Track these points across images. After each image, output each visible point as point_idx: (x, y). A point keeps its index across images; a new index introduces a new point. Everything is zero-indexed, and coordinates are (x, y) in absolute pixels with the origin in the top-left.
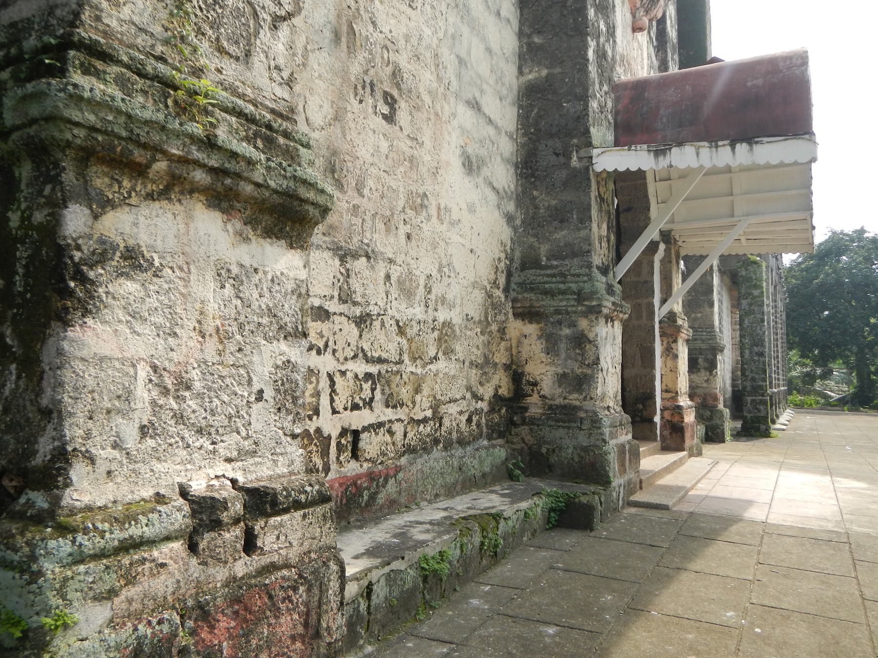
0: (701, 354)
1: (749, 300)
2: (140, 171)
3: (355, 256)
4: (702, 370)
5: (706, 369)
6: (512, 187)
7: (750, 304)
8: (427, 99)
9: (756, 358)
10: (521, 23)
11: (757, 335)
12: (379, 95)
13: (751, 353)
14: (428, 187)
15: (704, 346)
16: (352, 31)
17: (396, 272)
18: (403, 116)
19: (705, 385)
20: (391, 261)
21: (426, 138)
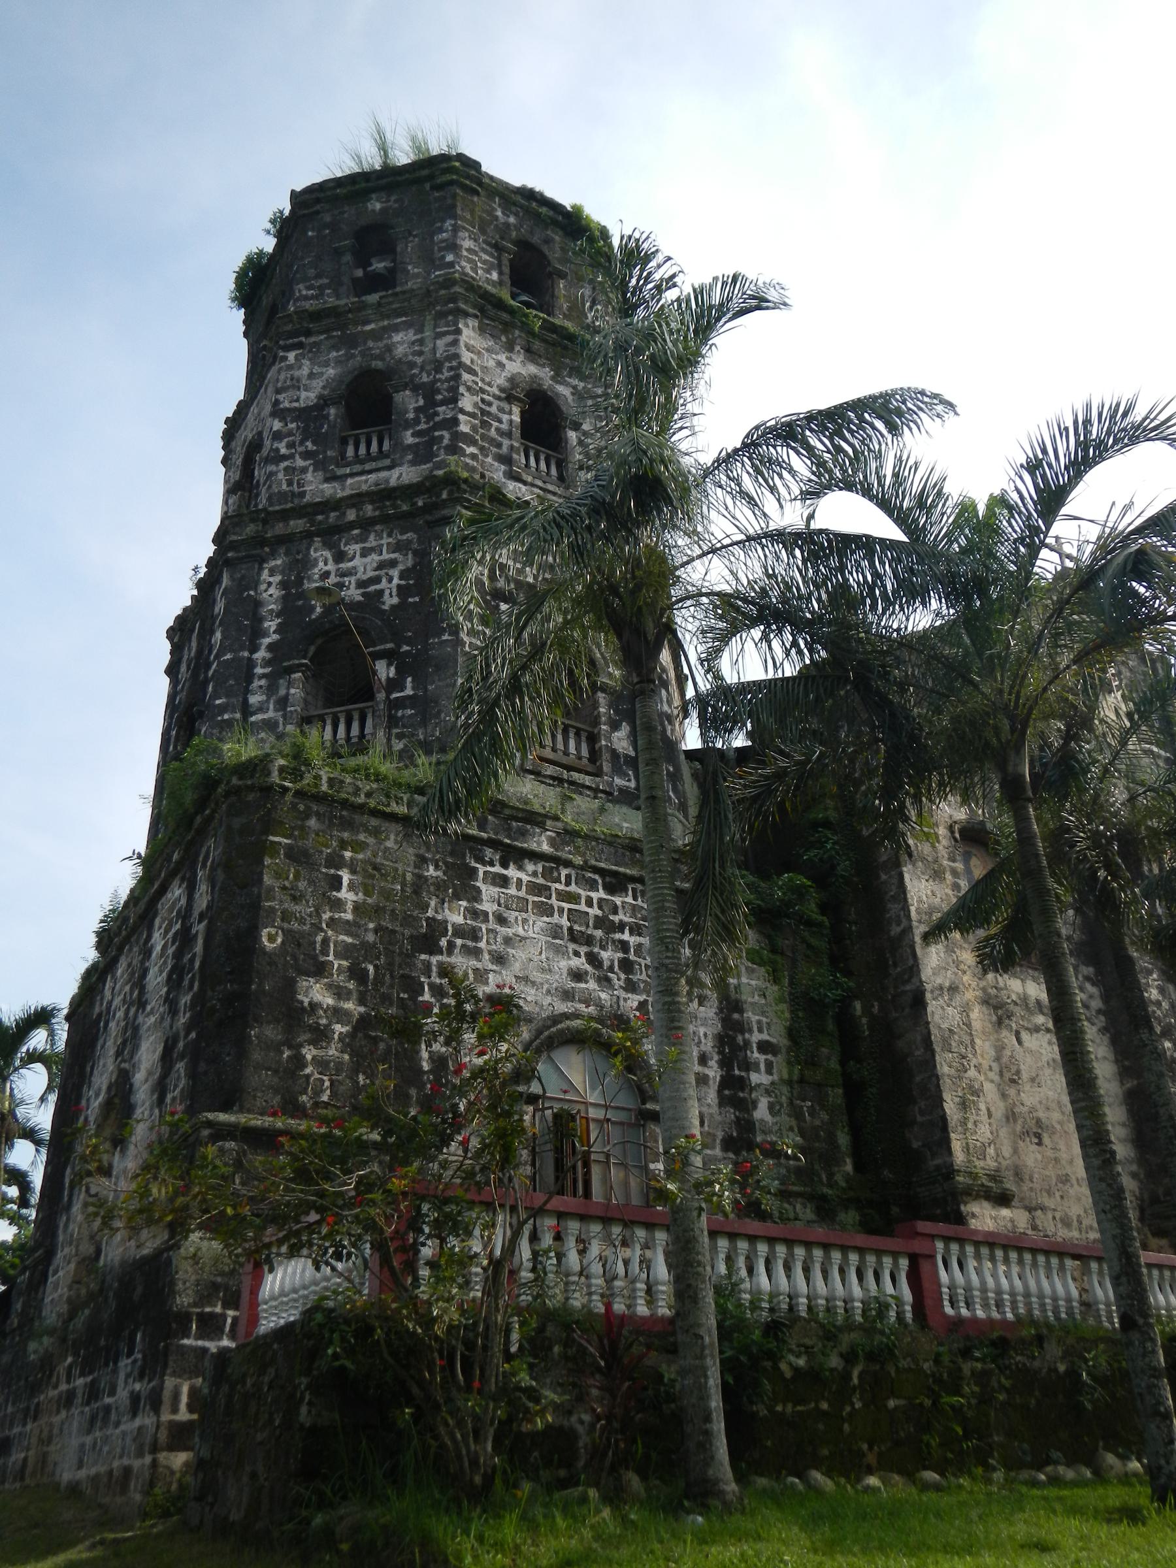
2: (970, 1195)
3: (1035, 1209)
6: (1132, 1155)
8: (1058, 1127)
10: (1116, 1054)
12: (1031, 1134)
14: (1069, 1171)
16: (1013, 1113)
17: (1058, 1215)
18: (1046, 1139)
20: (1054, 1210)
21: (1062, 1147)
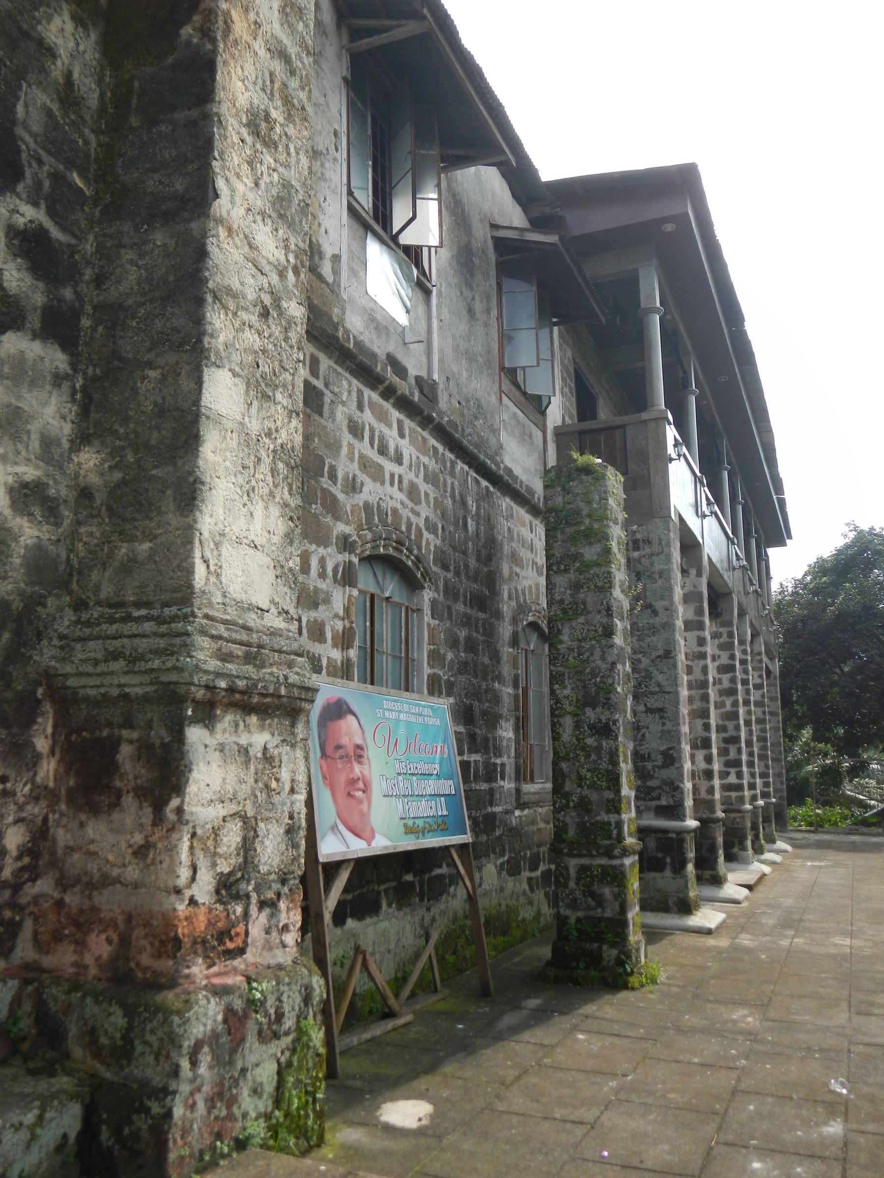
0: (128, 724)
1: (572, 575)
4: (129, 800)
5: (141, 793)
7: (576, 587)
9: (590, 741)
11: (594, 674)
13: (577, 726)
15: (136, 686)
19: (132, 873)
